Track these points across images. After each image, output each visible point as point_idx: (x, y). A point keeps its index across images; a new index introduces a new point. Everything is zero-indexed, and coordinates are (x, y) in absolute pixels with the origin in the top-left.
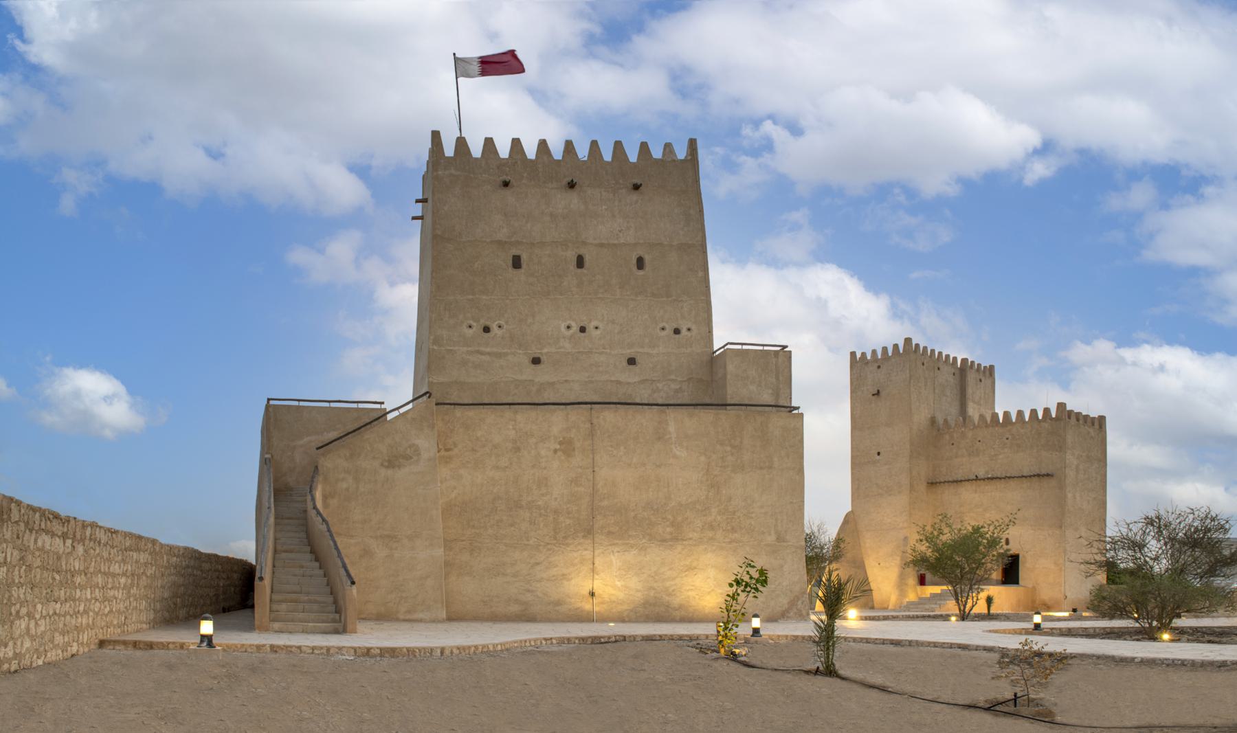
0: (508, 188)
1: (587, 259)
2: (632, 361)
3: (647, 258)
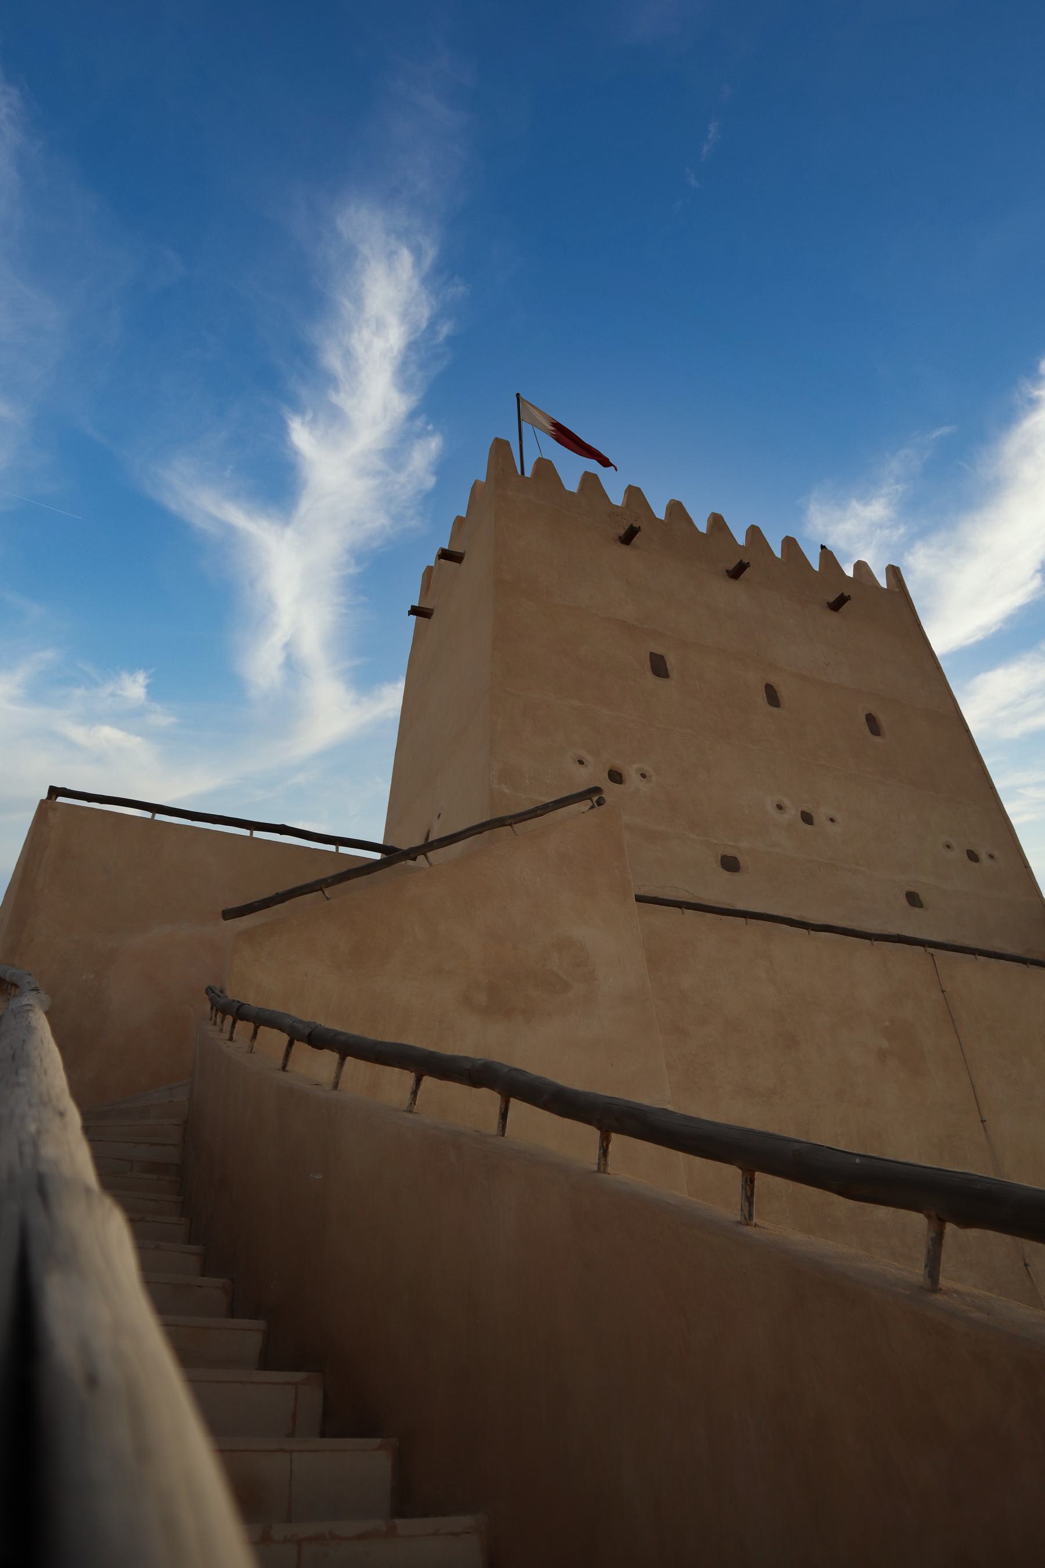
0: (628, 546)
1: (783, 693)
2: (913, 899)
3: (882, 718)
